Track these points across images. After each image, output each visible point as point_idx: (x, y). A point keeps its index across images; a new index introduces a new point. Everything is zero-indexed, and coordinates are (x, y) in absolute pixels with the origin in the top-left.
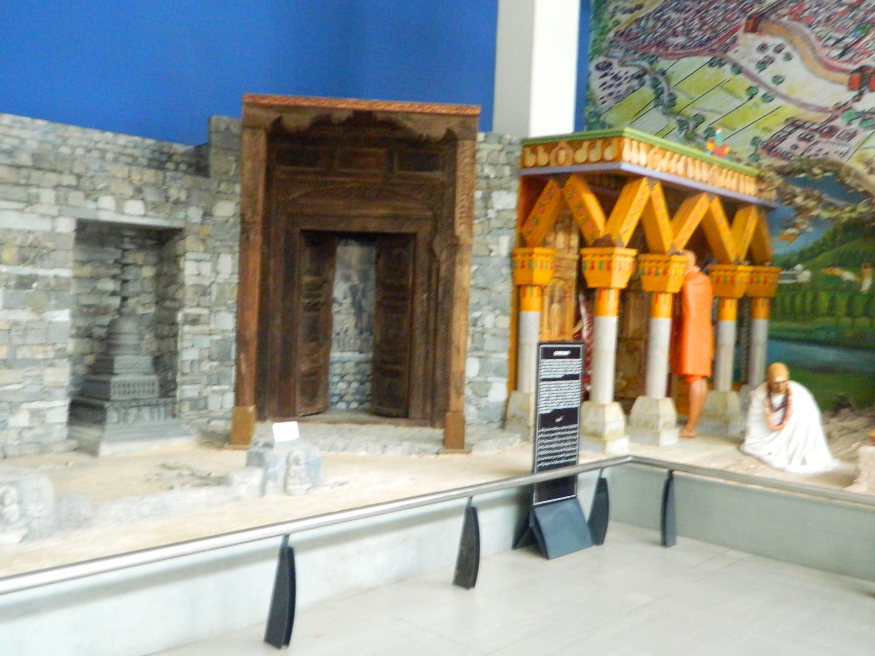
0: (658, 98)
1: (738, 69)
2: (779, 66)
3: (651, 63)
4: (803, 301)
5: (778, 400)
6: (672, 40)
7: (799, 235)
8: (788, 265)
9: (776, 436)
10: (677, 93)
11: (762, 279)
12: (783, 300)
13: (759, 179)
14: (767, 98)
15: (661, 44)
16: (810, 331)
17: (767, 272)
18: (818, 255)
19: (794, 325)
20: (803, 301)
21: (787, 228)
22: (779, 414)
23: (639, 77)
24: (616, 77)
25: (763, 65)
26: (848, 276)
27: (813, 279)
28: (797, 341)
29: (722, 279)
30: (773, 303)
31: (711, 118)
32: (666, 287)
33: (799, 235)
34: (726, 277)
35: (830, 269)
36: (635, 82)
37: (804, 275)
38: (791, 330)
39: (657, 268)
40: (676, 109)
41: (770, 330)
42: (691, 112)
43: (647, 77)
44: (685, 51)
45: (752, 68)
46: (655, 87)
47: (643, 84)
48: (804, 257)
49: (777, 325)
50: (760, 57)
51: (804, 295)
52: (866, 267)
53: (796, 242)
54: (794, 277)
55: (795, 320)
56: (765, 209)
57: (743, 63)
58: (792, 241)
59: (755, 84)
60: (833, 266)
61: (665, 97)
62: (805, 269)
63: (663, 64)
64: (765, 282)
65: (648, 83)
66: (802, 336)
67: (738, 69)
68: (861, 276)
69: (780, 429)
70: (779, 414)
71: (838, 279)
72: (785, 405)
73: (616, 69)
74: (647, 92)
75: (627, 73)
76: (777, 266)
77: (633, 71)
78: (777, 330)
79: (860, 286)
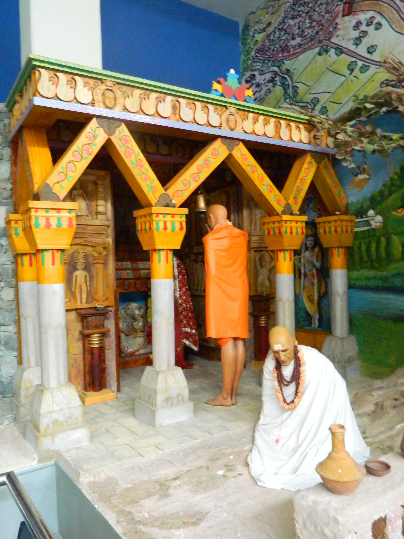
0: (286, 92)
1: (340, 50)
2: (373, 37)
3: (278, 67)
4: (378, 248)
5: (288, 372)
6: (293, 43)
7: (369, 179)
8: (361, 213)
9: (289, 416)
10: (298, 85)
11: (333, 229)
12: (359, 248)
13: (310, 126)
14: (364, 69)
15: (285, 49)
16: (386, 279)
17: (336, 221)
19: (372, 273)
20: (378, 248)
21: (356, 175)
22: (292, 387)
23: (272, 80)
24: (258, 85)
25: (358, 41)
27: (384, 223)
28: (376, 289)
30: (349, 251)
31: (323, 98)
32: (154, 245)
34: (274, 228)
35: (400, 211)
36: (270, 84)
37: (377, 221)
38: (369, 279)
40: (298, 98)
41: (349, 279)
42: (309, 98)
43: (277, 79)
44: (302, 48)
45: (353, 48)
46: (283, 85)
47: (275, 84)
48: (375, 202)
49: (355, 274)
50: (356, 34)
51: (378, 243)
53: (366, 186)
54: (368, 223)
55: (372, 267)
56: (319, 156)
57: (344, 44)
58: (363, 187)
59: (354, 60)
61: (290, 91)
62: (376, 214)
63: (288, 64)
64: (336, 231)
65: (279, 83)
66: (380, 283)
67: (340, 50)
69: (293, 409)
70: (292, 387)
72: (296, 376)
73: (259, 79)
74: (279, 90)
75: (265, 79)
76: (352, 214)
77: (268, 76)
78: (357, 279)
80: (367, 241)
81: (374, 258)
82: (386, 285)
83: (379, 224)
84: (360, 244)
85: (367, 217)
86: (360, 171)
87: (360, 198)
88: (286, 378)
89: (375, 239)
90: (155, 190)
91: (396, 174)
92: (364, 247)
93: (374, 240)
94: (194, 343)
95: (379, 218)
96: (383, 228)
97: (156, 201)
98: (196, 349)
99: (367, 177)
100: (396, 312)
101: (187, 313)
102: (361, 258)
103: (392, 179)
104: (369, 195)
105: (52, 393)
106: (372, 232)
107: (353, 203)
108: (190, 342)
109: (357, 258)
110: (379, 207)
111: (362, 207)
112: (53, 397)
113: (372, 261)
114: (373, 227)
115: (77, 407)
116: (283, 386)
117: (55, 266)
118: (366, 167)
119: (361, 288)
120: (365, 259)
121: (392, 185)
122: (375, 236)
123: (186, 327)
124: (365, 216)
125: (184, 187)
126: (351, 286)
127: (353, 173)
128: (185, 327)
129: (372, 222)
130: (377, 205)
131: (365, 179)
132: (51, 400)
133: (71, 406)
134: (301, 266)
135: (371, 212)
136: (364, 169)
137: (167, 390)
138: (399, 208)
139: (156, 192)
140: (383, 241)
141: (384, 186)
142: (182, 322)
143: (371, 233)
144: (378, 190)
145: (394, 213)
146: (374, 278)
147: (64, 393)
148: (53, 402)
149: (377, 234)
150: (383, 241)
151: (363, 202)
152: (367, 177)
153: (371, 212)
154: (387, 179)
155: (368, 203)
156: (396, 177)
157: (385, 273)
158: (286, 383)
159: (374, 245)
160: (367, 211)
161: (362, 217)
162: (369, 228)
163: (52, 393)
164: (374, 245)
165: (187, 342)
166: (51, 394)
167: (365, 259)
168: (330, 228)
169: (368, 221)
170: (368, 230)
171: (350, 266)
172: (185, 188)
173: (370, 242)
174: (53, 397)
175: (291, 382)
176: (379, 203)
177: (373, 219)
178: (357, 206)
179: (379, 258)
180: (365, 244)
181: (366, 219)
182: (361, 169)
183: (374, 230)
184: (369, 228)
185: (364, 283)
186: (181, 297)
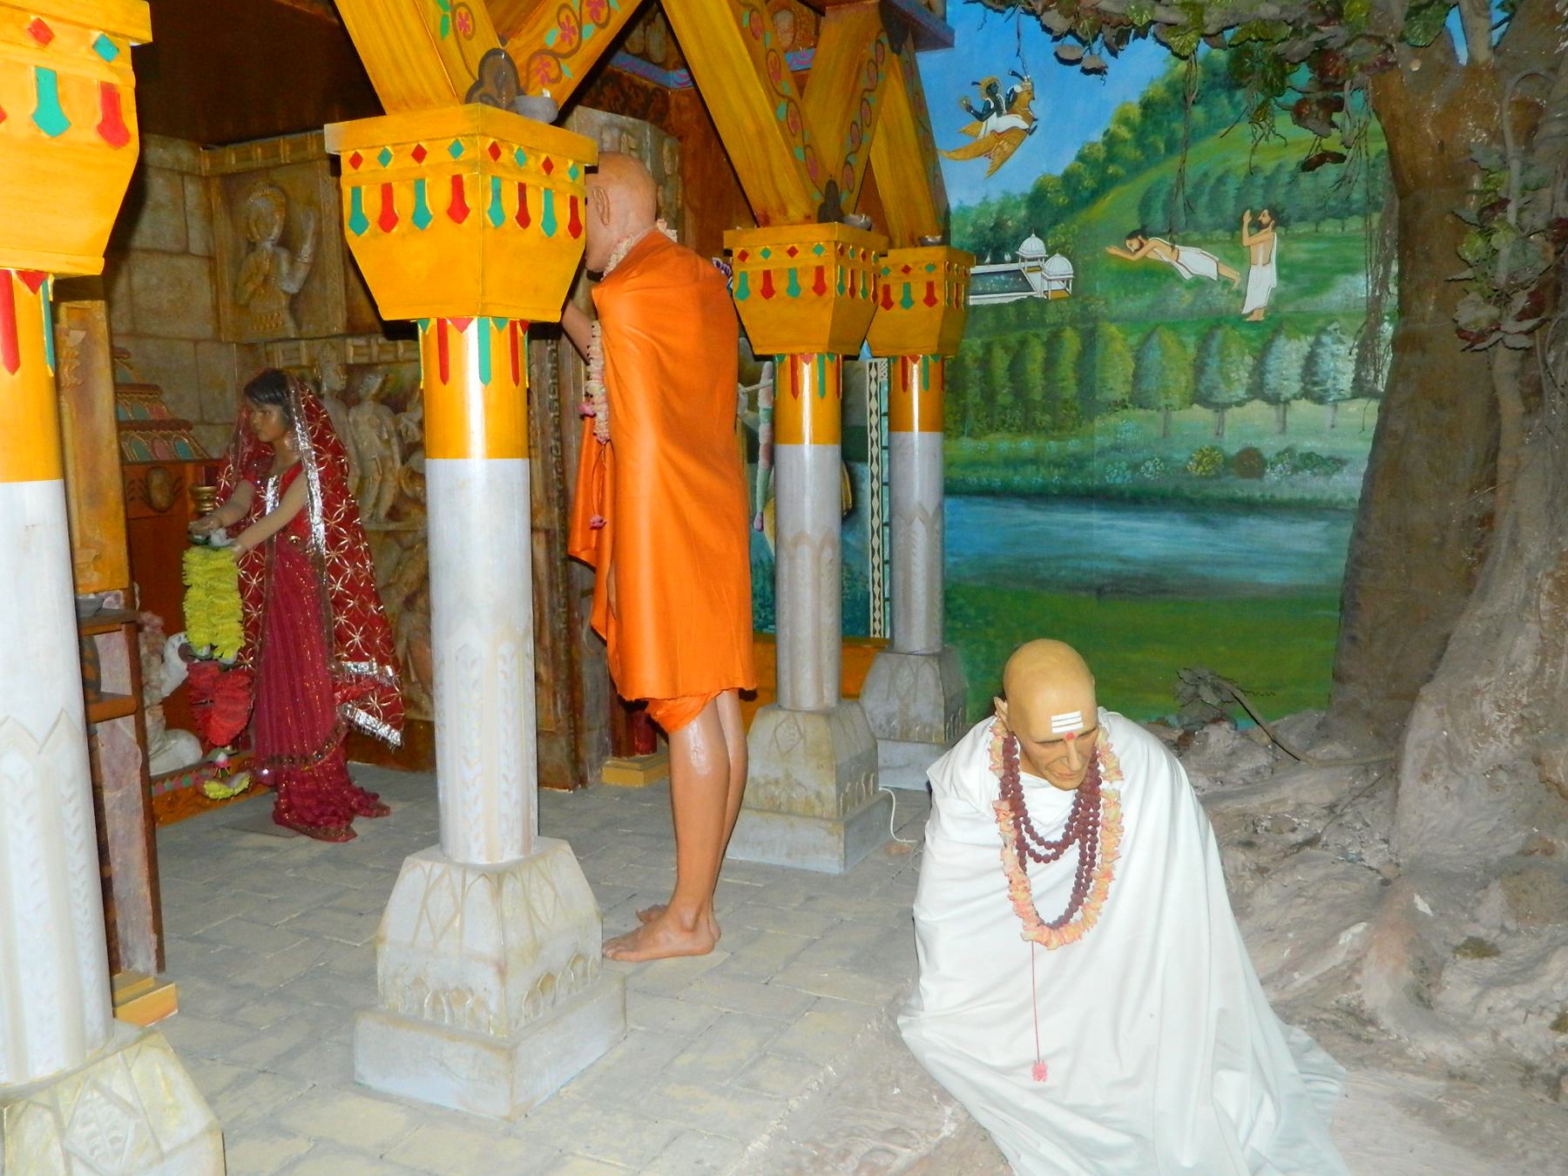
4: (1050, 364)
12: (985, 363)
18: (1096, 194)
20: (1050, 364)
21: (981, 117)
26: (1196, 262)
27: (1079, 284)
29: (780, 285)
33: (1030, 132)
34: (793, 273)
35: (1135, 244)
38: (1014, 462)
39: (419, 187)
41: (948, 464)
49: (966, 446)
51: (1053, 343)
52: (1257, 226)
54: (1019, 280)
55: (1028, 426)
58: (1005, 157)
60: (1143, 232)
62: (1051, 252)
66: (1056, 477)
68: (1243, 260)
71: (1162, 274)
72: (1085, 824)
78: (972, 464)
79: (1241, 295)
80: (1013, 338)
81: (1037, 395)
82: (1076, 481)
83: (1058, 286)
84: (988, 348)
85: (1015, 260)
86: (997, 103)
87: (995, 197)
88: (1041, 832)
89: (1045, 334)
90: (463, 25)
91: (1125, 121)
92: (1001, 361)
93: (1037, 336)
94: (388, 716)
95: (1060, 266)
96: (1074, 295)
97: (472, 82)
98: (395, 737)
99: (1024, 125)
100: (1108, 566)
101: (363, 604)
102: (989, 397)
103: (1111, 140)
104: (1028, 188)
105: (53, 1108)
106: (1032, 310)
107: (965, 211)
108: (370, 712)
109: (973, 395)
110: (1061, 227)
111: (999, 225)
112: (62, 1131)
113: (1029, 406)
114: (1038, 294)
115: (192, 1140)
116: (1030, 862)
117: (18, 373)
118: (1018, 89)
119: (988, 493)
120: (1004, 397)
121: (1111, 158)
122: (1043, 324)
123: (361, 658)
124: (1007, 257)
125: (563, 37)
126: (951, 489)
127: (969, 108)
128: (356, 657)
129: (1034, 279)
130: (1055, 223)
131: (1013, 129)
132: (56, 1149)
133: (166, 1147)
134: (757, 423)
135: (1032, 246)
136: (1012, 98)
137: (537, 948)
138: (1132, 235)
139: (469, 38)
140: (1071, 342)
141: (1081, 158)
142: (341, 637)
143: (1029, 314)
144: (1059, 172)
145: (1113, 250)
146: (1034, 461)
147: (120, 1087)
148: (67, 1156)
149: (1051, 318)
150: (1071, 342)
151: (1001, 211)
152: (1024, 125)
153: (1032, 246)
154: (1097, 137)
155: (1023, 213)
156: (1124, 133)
157: (1073, 445)
158: (1041, 851)
159: (1037, 352)
160: (1018, 240)
161: (997, 260)
162: (1024, 295)
163: (53, 1108)
164: (1037, 352)
165: (362, 718)
166: (48, 1116)
167: (1004, 397)
168: (907, 288)
169: (1018, 273)
170: (1020, 302)
171: (949, 418)
172: (566, 48)
173: (1023, 343)
174: (62, 1131)
175: (1060, 847)
176: (1060, 215)
177: (1039, 269)
178: (981, 221)
179: (1051, 395)
180: (1006, 349)
181: (1014, 267)
182: (1001, 97)
183: (1041, 303)
184: (1024, 295)
185: (997, 478)
186: (333, 539)
